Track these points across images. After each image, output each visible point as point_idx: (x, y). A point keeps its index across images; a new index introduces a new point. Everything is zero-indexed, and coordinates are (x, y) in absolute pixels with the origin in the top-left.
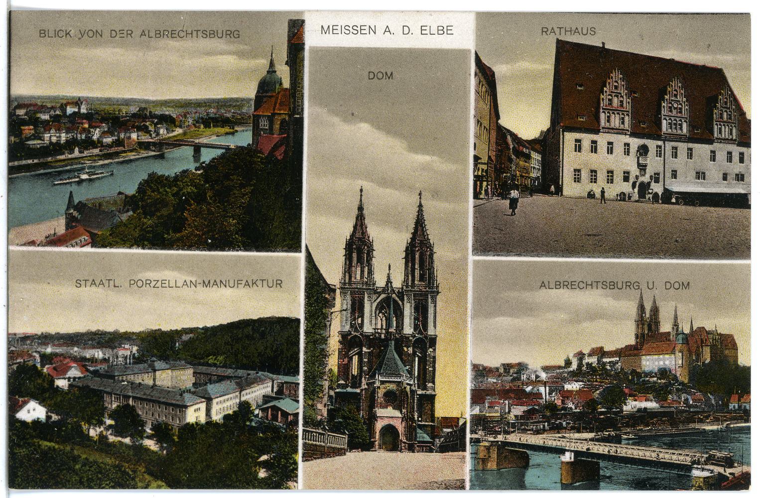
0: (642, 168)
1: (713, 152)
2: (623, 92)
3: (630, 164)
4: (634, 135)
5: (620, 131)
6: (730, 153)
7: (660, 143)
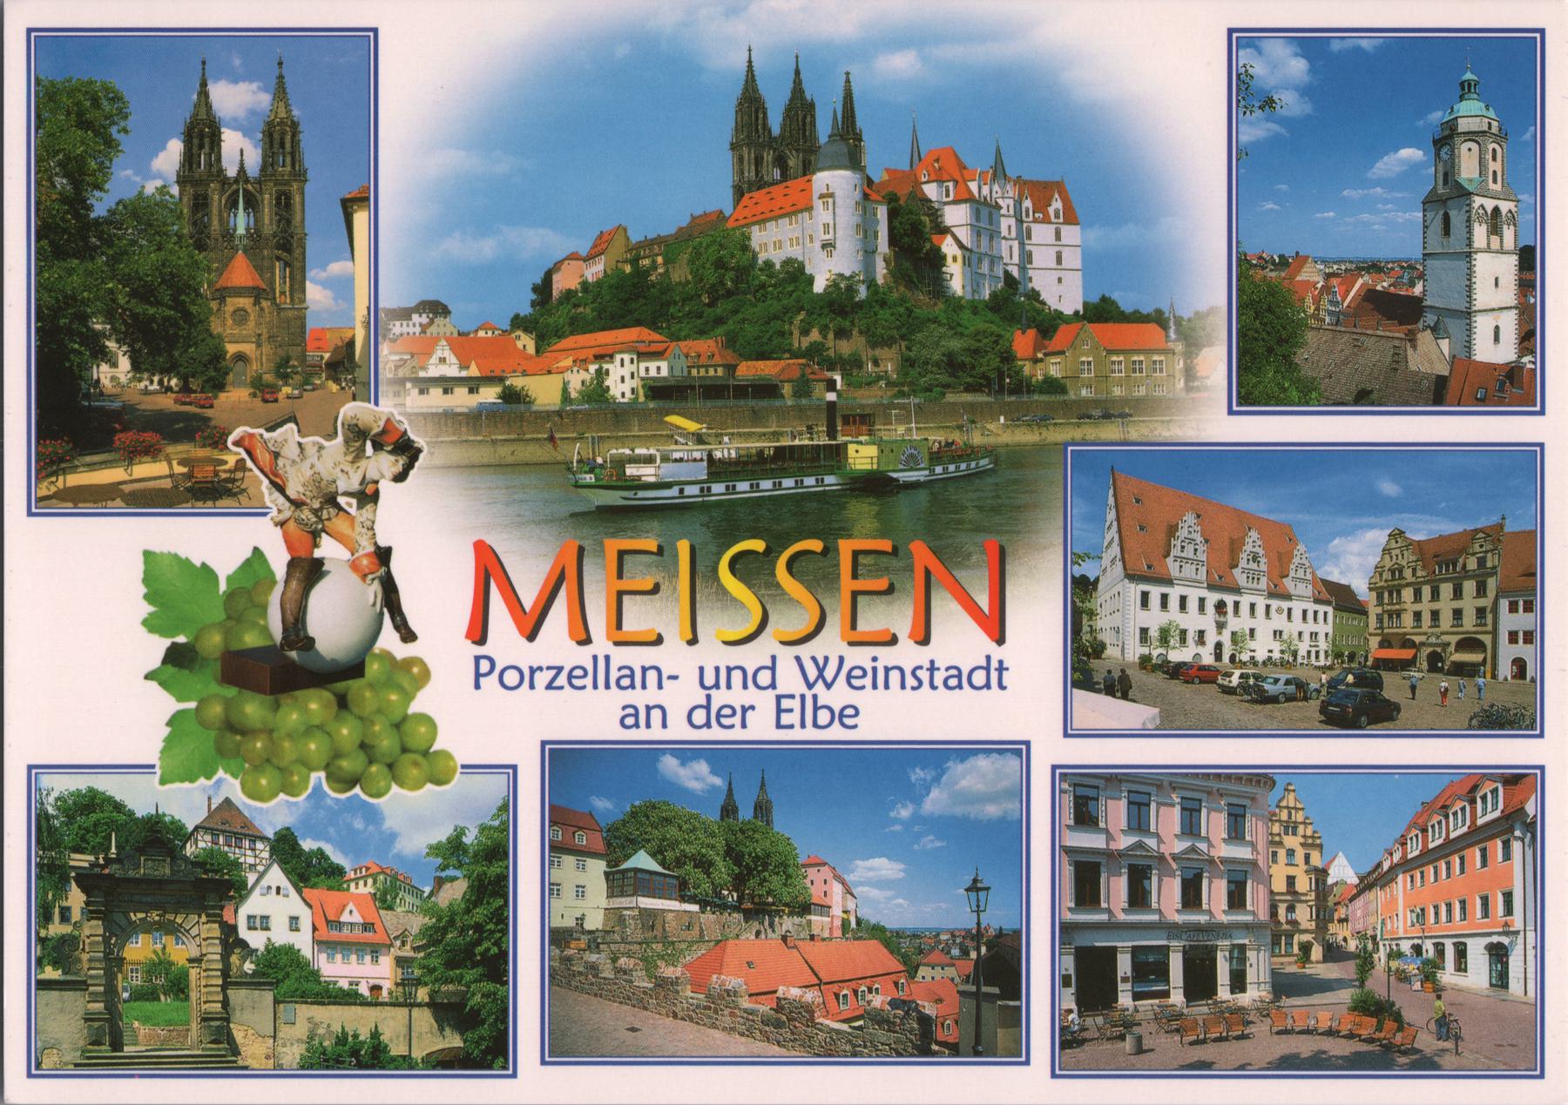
0: (1221, 626)
1: (1290, 610)
2: (1199, 538)
4: (1212, 587)
5: (1193, 583)
6: (1305, 612)
7: (1237, 598)
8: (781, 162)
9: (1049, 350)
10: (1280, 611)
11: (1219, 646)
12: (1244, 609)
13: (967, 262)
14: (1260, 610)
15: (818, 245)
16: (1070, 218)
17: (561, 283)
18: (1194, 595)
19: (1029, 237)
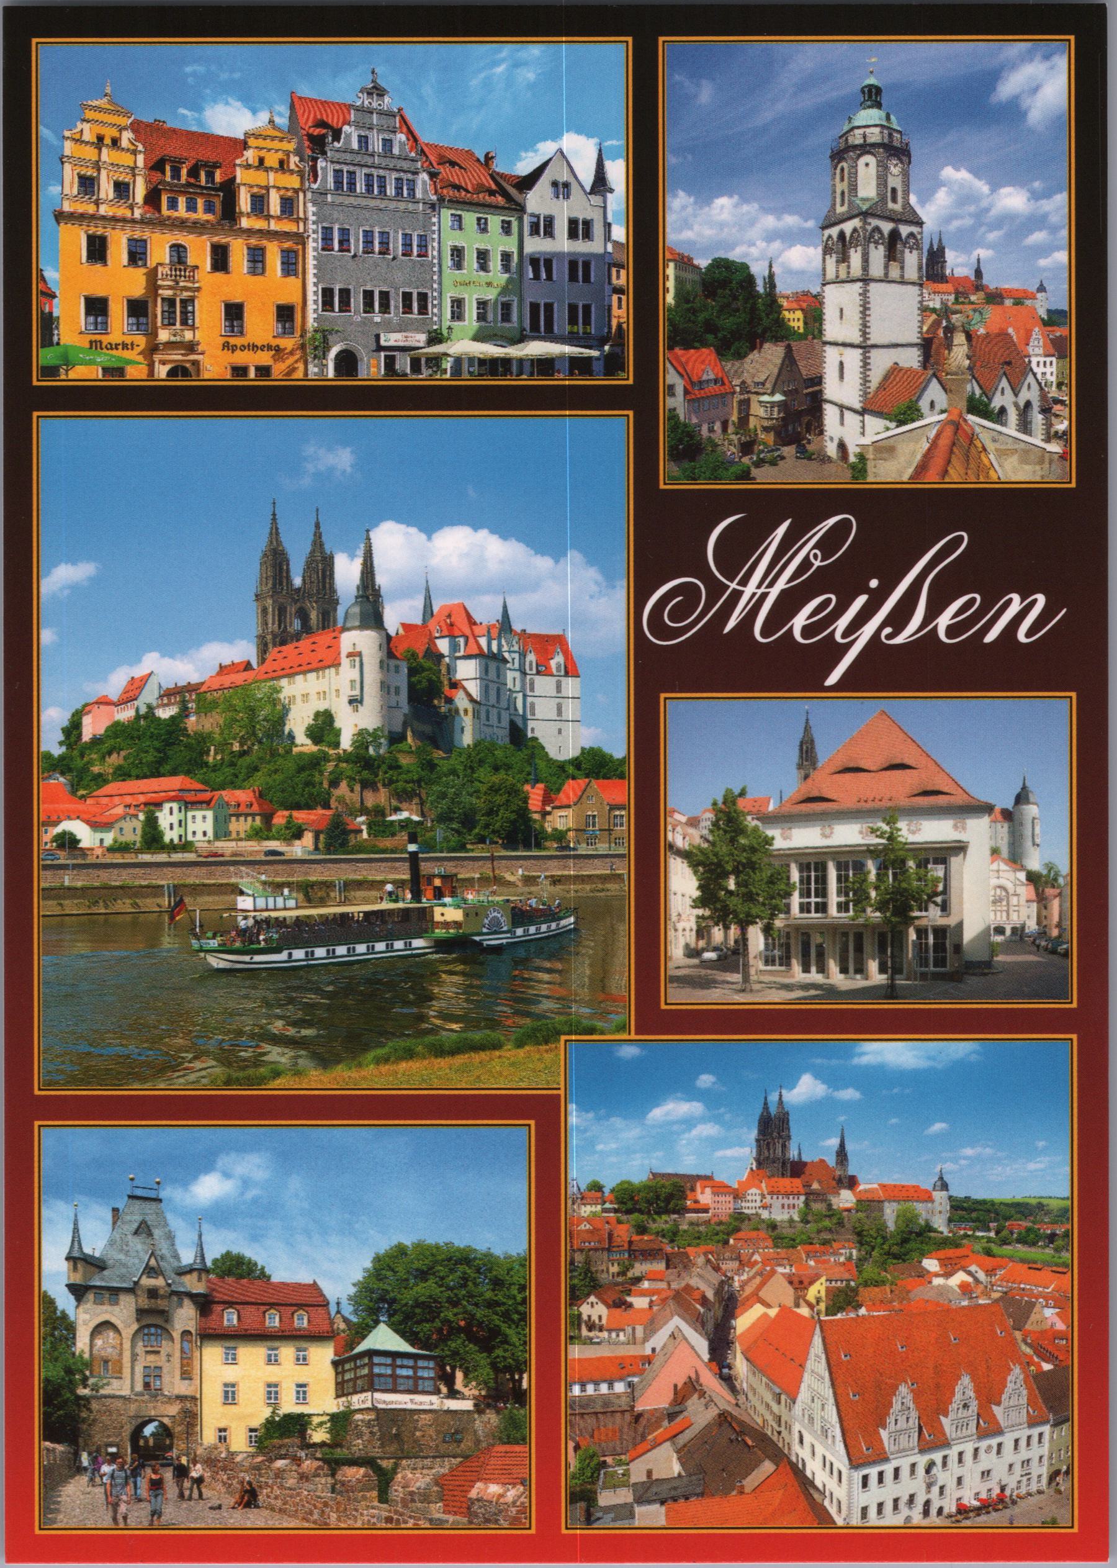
8: (303, 616)
9: (557, 803)
13: (476, 715)
15: (346, 700)
16: (570, 670)
17: (90, 728)
19: (532, 690)
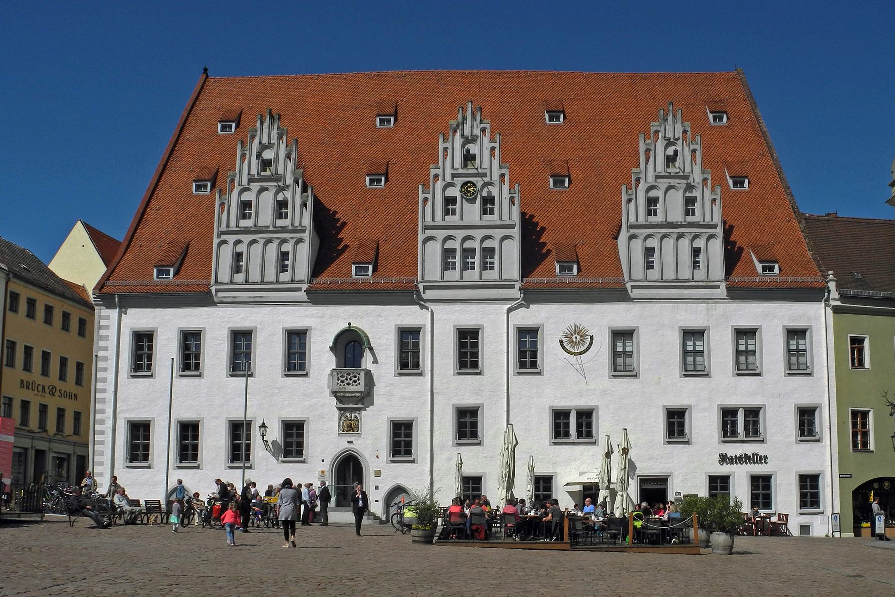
3: (311, 398)
4: (318, 296)
5: (260, 293)
10: (577, 342)
11: (349, 467)
12: (440, 350)
14: (497, 349)
18: (269, 325)
